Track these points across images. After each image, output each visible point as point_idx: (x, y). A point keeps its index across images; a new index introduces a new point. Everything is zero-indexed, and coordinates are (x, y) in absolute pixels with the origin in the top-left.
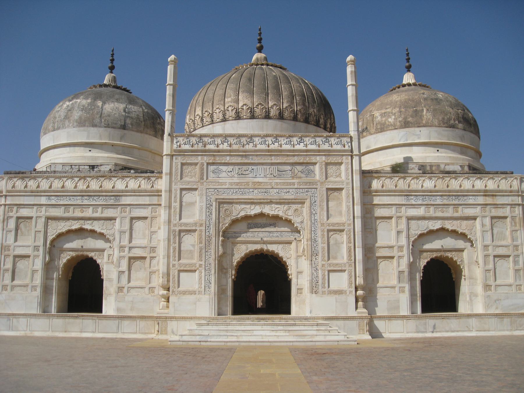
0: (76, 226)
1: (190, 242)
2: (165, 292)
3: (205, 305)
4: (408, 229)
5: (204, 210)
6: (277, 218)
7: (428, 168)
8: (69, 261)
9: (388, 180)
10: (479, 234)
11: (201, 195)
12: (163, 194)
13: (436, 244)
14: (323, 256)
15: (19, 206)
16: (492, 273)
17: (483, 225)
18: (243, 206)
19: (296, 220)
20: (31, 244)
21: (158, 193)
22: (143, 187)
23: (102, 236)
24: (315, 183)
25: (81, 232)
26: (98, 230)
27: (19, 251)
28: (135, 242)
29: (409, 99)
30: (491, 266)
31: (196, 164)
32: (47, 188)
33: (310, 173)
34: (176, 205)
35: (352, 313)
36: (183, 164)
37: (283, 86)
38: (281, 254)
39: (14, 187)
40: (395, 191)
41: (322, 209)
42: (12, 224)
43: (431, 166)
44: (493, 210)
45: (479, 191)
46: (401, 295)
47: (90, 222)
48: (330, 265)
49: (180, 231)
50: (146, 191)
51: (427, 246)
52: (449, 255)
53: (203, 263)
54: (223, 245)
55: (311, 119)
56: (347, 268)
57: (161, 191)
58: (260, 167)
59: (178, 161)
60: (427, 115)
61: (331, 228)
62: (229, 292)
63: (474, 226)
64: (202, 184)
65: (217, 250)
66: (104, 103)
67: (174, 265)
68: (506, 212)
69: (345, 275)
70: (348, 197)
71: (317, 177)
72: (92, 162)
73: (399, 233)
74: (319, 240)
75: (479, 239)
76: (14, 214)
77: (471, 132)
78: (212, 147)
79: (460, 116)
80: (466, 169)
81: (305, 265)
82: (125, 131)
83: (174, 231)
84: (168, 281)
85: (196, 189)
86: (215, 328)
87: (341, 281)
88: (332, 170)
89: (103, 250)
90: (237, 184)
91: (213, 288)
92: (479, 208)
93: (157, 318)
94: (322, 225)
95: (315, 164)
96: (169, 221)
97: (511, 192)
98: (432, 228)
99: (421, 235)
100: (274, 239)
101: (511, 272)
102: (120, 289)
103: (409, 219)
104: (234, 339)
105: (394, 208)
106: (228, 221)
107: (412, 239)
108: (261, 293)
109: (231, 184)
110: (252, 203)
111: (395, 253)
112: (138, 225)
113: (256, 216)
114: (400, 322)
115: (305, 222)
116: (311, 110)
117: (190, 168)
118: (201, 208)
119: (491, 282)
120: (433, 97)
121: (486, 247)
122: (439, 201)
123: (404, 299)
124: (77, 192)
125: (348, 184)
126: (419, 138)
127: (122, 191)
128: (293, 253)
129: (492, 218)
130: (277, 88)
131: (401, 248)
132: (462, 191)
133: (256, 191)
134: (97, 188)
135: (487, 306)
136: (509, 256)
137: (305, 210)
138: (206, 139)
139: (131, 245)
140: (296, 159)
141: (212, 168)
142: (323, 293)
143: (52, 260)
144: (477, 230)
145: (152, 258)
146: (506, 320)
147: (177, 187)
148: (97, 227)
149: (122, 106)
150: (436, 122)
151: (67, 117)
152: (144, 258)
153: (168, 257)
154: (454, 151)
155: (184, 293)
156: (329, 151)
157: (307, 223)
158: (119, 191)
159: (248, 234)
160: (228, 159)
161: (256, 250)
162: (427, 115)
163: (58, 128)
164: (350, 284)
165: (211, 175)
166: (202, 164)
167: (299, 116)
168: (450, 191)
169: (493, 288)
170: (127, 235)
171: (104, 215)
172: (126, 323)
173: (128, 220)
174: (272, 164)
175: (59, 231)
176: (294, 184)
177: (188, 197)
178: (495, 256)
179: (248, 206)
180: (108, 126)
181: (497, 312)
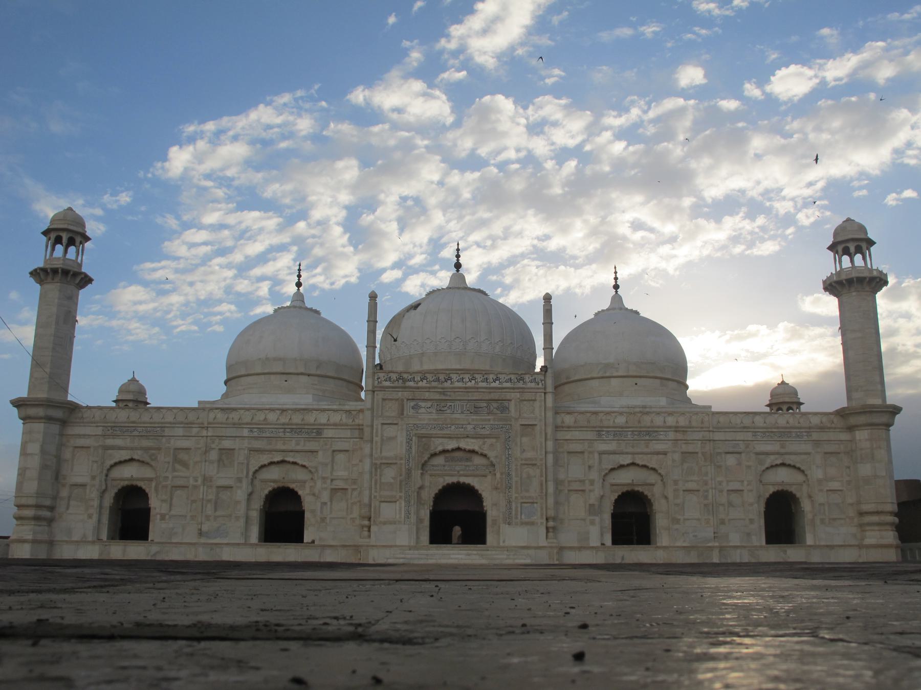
1: (389, 474)
13: (626, 478)
17: (674, 461)
18: (440, 440)
19: (491, 454)
22: (344, 420)
26: (300, 462)
33: (504, 409)
35: (543, 542)
38: (477, 487)
42: (214, 455)
44: (684, 446)
45: (670, 427)
47: (291, 454)
48: (522, 498)
52: (640, 489)
53: (403, 494)
58: (457, 403)
59: (380, 395)
61: (524, 462)
62: (427, 522)
67: (375, 497)
71: (513, 412)
73: (590, 467)
74: (514, 474)
78: (411, 384)
83: (376, 464)
84: (370, 511)
86: (416, 552)
89: (305, 482)
90: (435, 420)
91: (413, 518)
95: (510, 400)
96: (371, 455)
98: (622, 463)
103: (601, 453)
108: (457, 531)
109: (430, 419)
112: (340, 457)
113: (453, 450)
131: (592, 482)
132: (653, 427)
133: (453, 427)
140: (493, 396)
141: (412, 404)
145: (353, 490)
152: (346, 489)
153: (371, 489)
155: (385, 523)
158: (321, 425)
161: (453, 483)
164: (542, 515)
170: (329, 467)
171: (306, 448)
175: (262, 463)
176: (489, 420)
179: (445, 441)
181: (684, 545)
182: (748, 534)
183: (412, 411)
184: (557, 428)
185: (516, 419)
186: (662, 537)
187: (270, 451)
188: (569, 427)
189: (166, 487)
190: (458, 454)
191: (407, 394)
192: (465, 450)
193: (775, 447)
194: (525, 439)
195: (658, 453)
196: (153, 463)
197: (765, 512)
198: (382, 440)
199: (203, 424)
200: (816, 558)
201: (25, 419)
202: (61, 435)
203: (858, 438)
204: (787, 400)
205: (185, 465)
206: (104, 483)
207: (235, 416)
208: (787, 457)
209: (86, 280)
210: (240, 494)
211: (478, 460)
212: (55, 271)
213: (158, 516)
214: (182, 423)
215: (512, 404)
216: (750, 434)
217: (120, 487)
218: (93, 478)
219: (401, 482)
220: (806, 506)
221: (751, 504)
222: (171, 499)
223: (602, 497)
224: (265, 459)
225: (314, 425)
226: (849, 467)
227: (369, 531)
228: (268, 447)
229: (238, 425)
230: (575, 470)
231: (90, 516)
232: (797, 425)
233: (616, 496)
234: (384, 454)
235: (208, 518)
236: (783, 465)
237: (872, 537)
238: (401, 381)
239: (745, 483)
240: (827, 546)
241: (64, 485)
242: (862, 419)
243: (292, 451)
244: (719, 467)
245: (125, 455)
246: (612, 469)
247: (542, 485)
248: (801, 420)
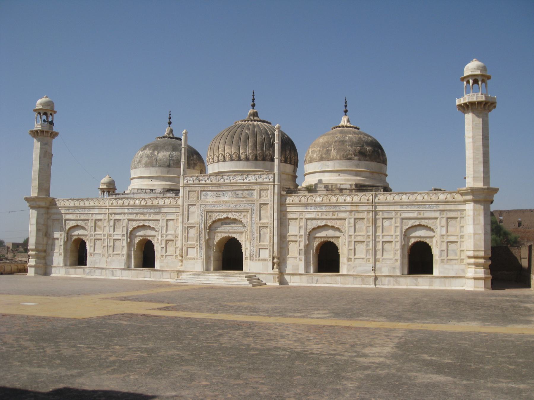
0: (141, 224)
1: (192, 232)
2: (181, 258)
3: (199, 265)
4: (306, 225)
6: (235, 219)
7: (330, 187)
8: (139, 241)
9: (296, 197)
10: (347, 229)
11: (198, 208)
14: (257, 240)
16: (353, 251)
17: (349, 223)
18: (218, 213)
19: (244, 221)
20: (121, 233)
21: (177, 207)
23: (153, 229)
25: (144, 227)
27: (116, 237)
28: (169, 232)
29: (327, 142)
30: (352, 247)
31: (196, 191)
34: (186, 213)
35: (270, 271)
36: (189, 192)
37: (250, 140)
39: (112, 204)
41: (257, 215)
42: (112, 223)
43: (332, 186)
45: (348, 203)
46: (300, 262)
48: (260, 245)
49: (188, 227)
51: (318, 235)
52: (331, 240)
54: (208, 234)
55: (267, 158)
56: (268, 247)
59: (186, 190)
60: (333, 153)
61: (261, 225)
63: (344, 224)
65: (205, 237)
66: (158, 153)
67: (185, 245)
68: (364, 215)
69: (267, 251)
70: (271, 208)
71: (255, 197)
72: (152, 188)
74: (255, 232)
75: (347, 231)
77: (367, 160)
78: (203, 182)
79: (357, 151)
80: (354, 187)
81: (248, 246)
82: (170, 168)
83: (185, 227)
84: (182, 252)
85: (195, 205)
87: (265, 254)
88: (263, 193)
89: (155, 236)
90: (215, 202)
91: (203, 256)
92: (348, 213)
93: (177, 271)
94: (257, 223)
95: (255, 190)
97: (368, 203)
98: (320, 225)
99: (314, 229)
100: (234, 231)
101: (365, 251)
102: (162, 256)
103: (307, 220)
104: (199, 282)
105: (298, 214)
107: (308, 231)
109: (212, 202)
111: (298, 239)
112: (170, 223)
114: (298, 277)
116: (267, 152)
117: (193, 193)
118: (198, 216)
119: (352, 256)
120: (342, 139)
121: (350, 236)
123: (301, 265)
125: (271, 201)
126: (328, 167)
127: (162, 206)
128: (244, 238)
129: (355, 219)
130: (246, 142)
131: (301, 236)
134: (150, 204)
135: (348, 270)
136: (364, 242)
137: (249, 216)
139: (167, 234)
140: (244, 188)
141: (203, 193)
142: (256, 260)
143: (131, 241)
144: (346, 226)
145: (177, 240)
146: (359, 279)
147: (186, 204)
148: (151, 224)
149: (168, 153)
150: (338, 157)
151: (140, 162)
152: (173, 240)
154: (350, 174)
155: (190, 259)
156: (262, 183)
157: (249, 223)
158: (161, 206)
159: (222, 228)
160: (211, 188)
162: (333, 153)
163: (136, 168)
164: (270, 255)
165: (203, 197)
166: (198, 191)
167: (259, 158)
168: (331, 203)
169: (353, 260)
170: (165, 228)
172: (164, 273)
173: (165, 221)
177: (192, 209)
178: (355, 242)
179: (220, 214)
180: (160, 166)
185: (257, 201)
186: (343, 269)
187: (138, 220)
190: (227, 221)
191: (200, 189)
193: (415, 215)
195: (341, 219)
196: (86, 227)
205: (100, 227)
208: (423, 220)
209: (54, 135)
210: (125, 244)
214: (98, 206)
215: (256, 191)
216: (399, 206)
219: (197, 236)
224: (135, 224)
228: (137, 218)
231: (60, 254)
232: (429, 200)
235: (110, 255)
236: (420, 225)
239: (394, 237)
240: (445, 277)
247: (270, 238)
248: (433, 197)
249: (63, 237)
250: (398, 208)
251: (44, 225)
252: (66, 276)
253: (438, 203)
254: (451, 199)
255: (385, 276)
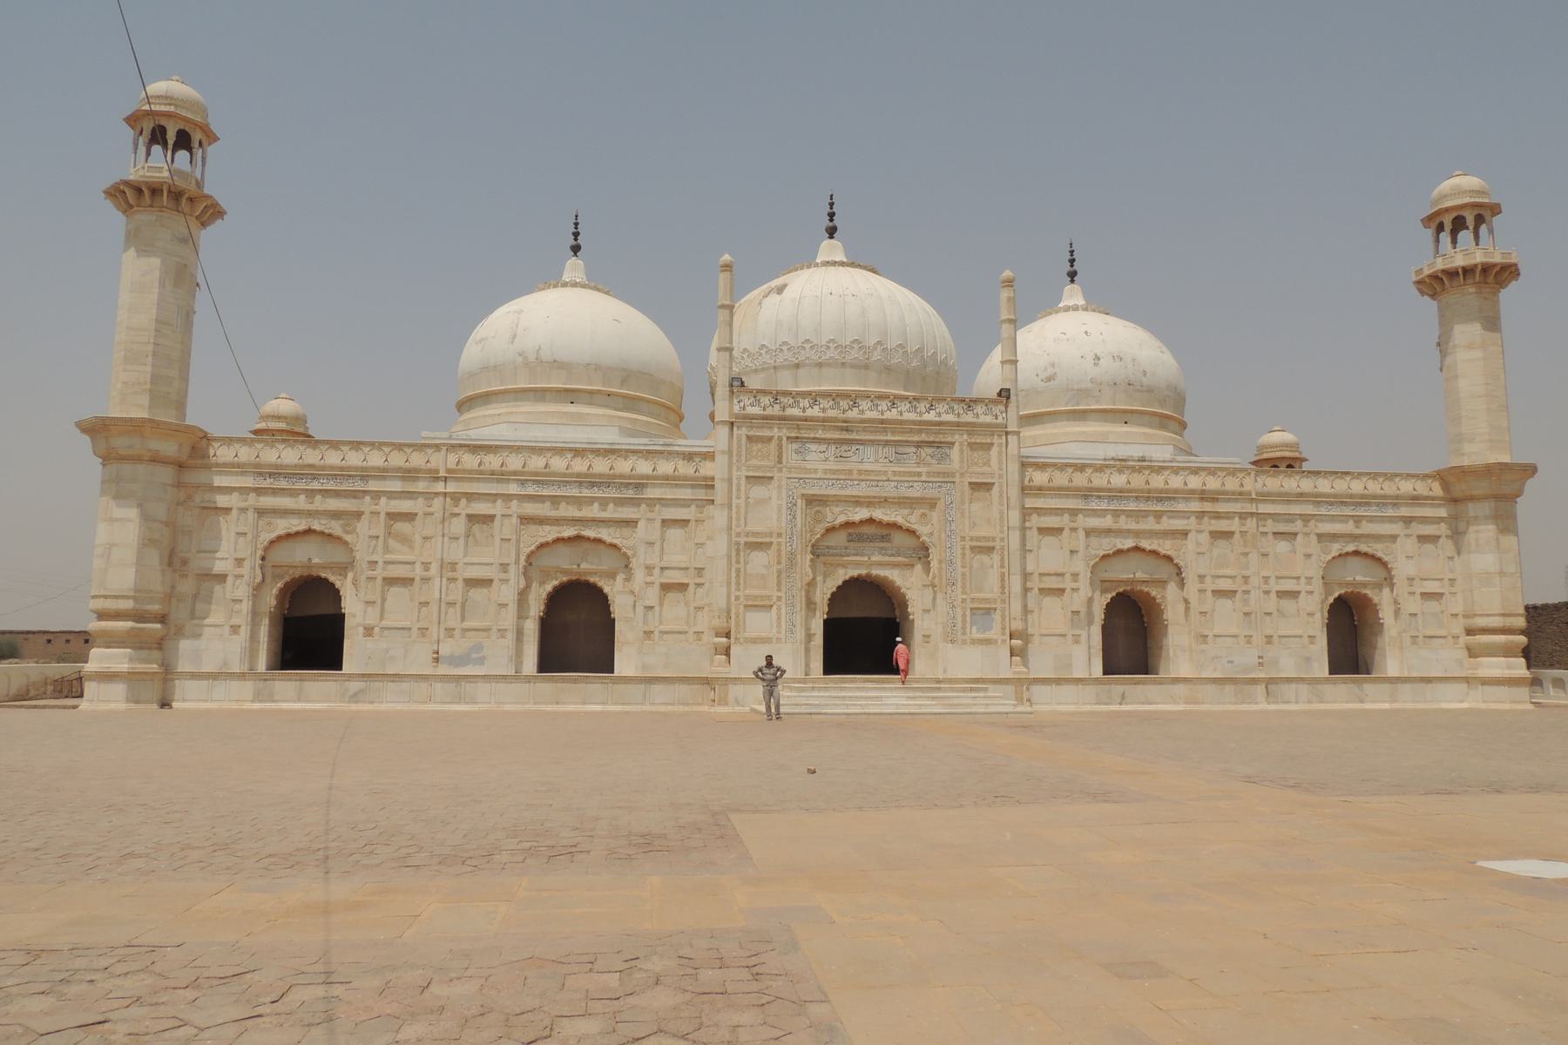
0: (569, 532)
5: (784, 510)
12: (718, 484)
14: (964, 587)
15: (471, 497)
17: (1198, 544)
19: (923, 530)
24: (953, 474)
26: (608, 540)
31: (770, 439)
32: (520, 468)
40: (1068, 489)
42: (458, 526)
45: (1193, 492)
50: (686, 478)
57: (713, 479)
64: (780, 470)
68: (1234, 525)
76: (465, 508)
78: (795, 412)
83: (738, 543)
91: (800, 634)
94: (963, 539)
96: (730, 528)
98: (1120, 546)
106: (820, 529)
109: (825, 472)
110: (857, 502)
112: (675, 534)
113: (861, 522)
115: (936, 534)
118: (780, 510)
122: (1132, 506)
124: (572, 475)
125: (1000, 476)
126: (1097, 402)
127: (648, 477)
131: (1075, 576)
132: (1167, 491)
138: (784, 400)
139: (664, 564)
140: (924, 437)
141: (795, 446)
145: (699, 585)
146: (1229, 689)
148: (605, 534)
153: (729, 583)
160: (820, 434)
166: (780, 439)
170: (657, 547)
172: (657, 688)
174: (887, 443)
175: (543, 540)
176: (919, 474)
182: (1308, 659)
183: (795, 456)
184: (1025, 490)
188: (1040, 489)
189: (373, 579)
192: (880, 523)
193: (1349, 527)
194: (974, 507)
196: (348, 538)
197: (1328, 626)
198: (747, 504)
199: (437, 471)
200: (1409, 700)
201: (107, 458)
202: (179, 485)
203: (1472, 514)
204: (1287, 454)
205: (405, 540)
206: (258, 572)
207: (493, 461)
209: (212, 212)
211: (898, 539)
212: (155, 191)
213: (361, 629)
214: (398, 469)
217: (287, 579)
218: (239, 562)
219: (779, 572)
220: (1386, 614)
221: (1311, 614)
222: (384, 600)
223: (1090, 601)
224: (549, 533)
225: (630, 477)
226: (1451, 558)
227: (727, 652)
229: (500, 476)
230: (1049, 556)
231: (235, 629)
233: (1109, 596)
234: (749, 528)
236: (1356, 553)
237: (1495, 667)
238: (777, 407)
241: (185, 576)
242: (1481, 487)
243: (594, 520)
244: (1265, 555)
245: (298, 525)
246: (1104, 557)
249: (245, 569)
250: (1309, 509)
251: (166, 524)
252: (257, 706)
253: (1397, 500)
254: (1426, 493)
255: (1289, 680)
